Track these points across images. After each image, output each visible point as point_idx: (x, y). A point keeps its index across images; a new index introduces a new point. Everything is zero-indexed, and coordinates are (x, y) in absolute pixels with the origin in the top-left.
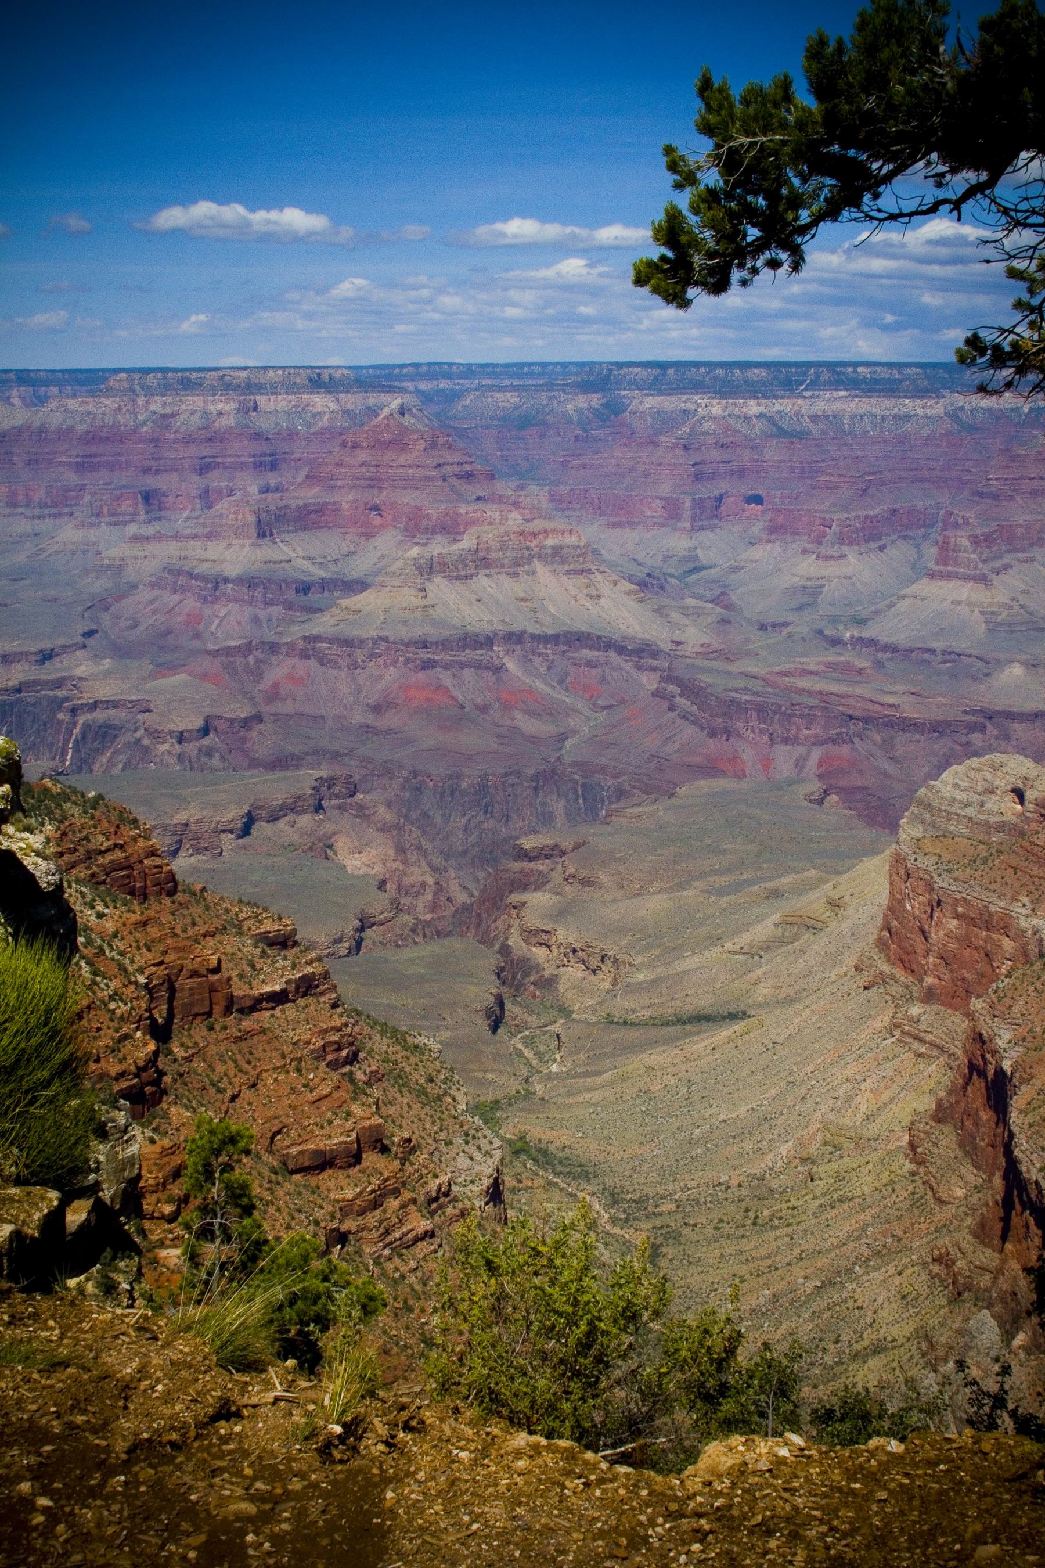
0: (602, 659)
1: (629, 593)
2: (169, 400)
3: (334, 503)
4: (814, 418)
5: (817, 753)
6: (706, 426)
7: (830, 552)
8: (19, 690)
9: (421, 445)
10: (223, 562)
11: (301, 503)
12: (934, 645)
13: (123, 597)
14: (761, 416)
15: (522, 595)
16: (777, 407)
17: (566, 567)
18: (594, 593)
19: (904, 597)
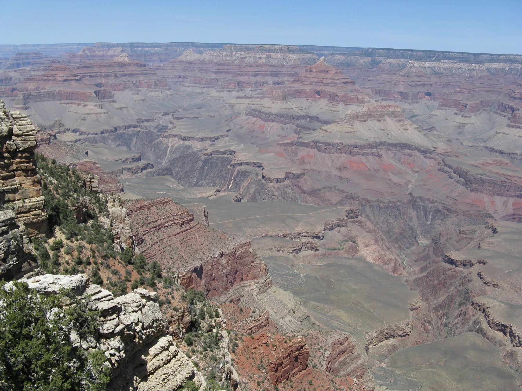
0: (413, 154)
1: (415, 128)
2: (243, 53)
3: (305, 90)
4: (444, 69)
5: (511, 200)
6: (413, 70)
7: (467, 115)
8: (211, 154)
9: (333, 72)
10: (271, 108)
11: (294, 89)
12: (516, 152)
13: (236, 117)
14: (429, 67)
15: (383, 128)
16: (433, 65)
17: (396, 119)
18: (405, 128)
19: (499, 133)
